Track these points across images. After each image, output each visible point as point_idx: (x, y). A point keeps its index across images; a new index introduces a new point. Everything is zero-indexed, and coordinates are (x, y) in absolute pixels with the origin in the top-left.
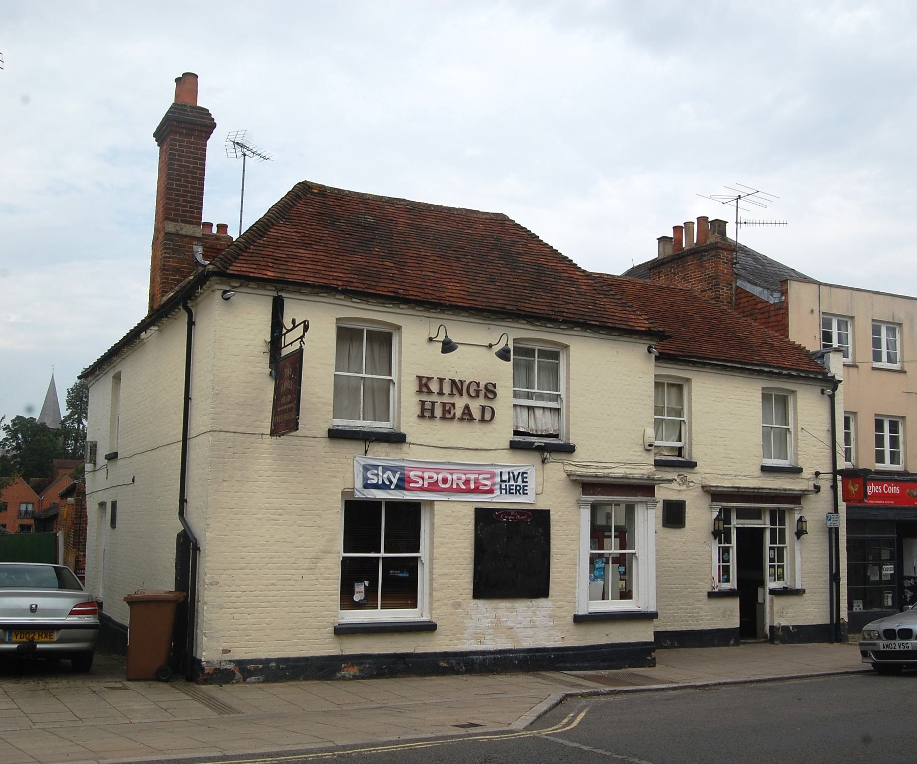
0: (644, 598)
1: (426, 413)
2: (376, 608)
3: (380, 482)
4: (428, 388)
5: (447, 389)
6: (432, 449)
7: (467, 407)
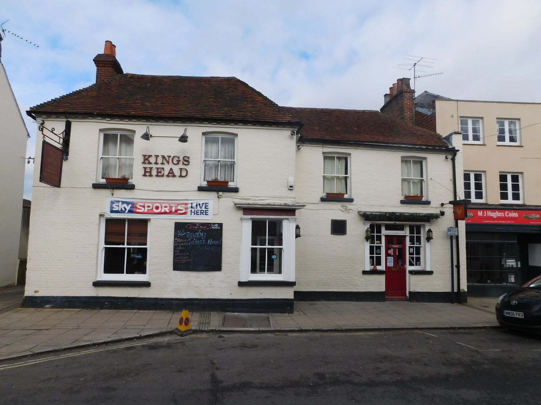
0: (288, 273)
1: (147, 173)
2: (123, 273)
3: (120, 210)
4: (149, 161)
5: (160, 160)
6: (147, 190)
7: (171, 169)
